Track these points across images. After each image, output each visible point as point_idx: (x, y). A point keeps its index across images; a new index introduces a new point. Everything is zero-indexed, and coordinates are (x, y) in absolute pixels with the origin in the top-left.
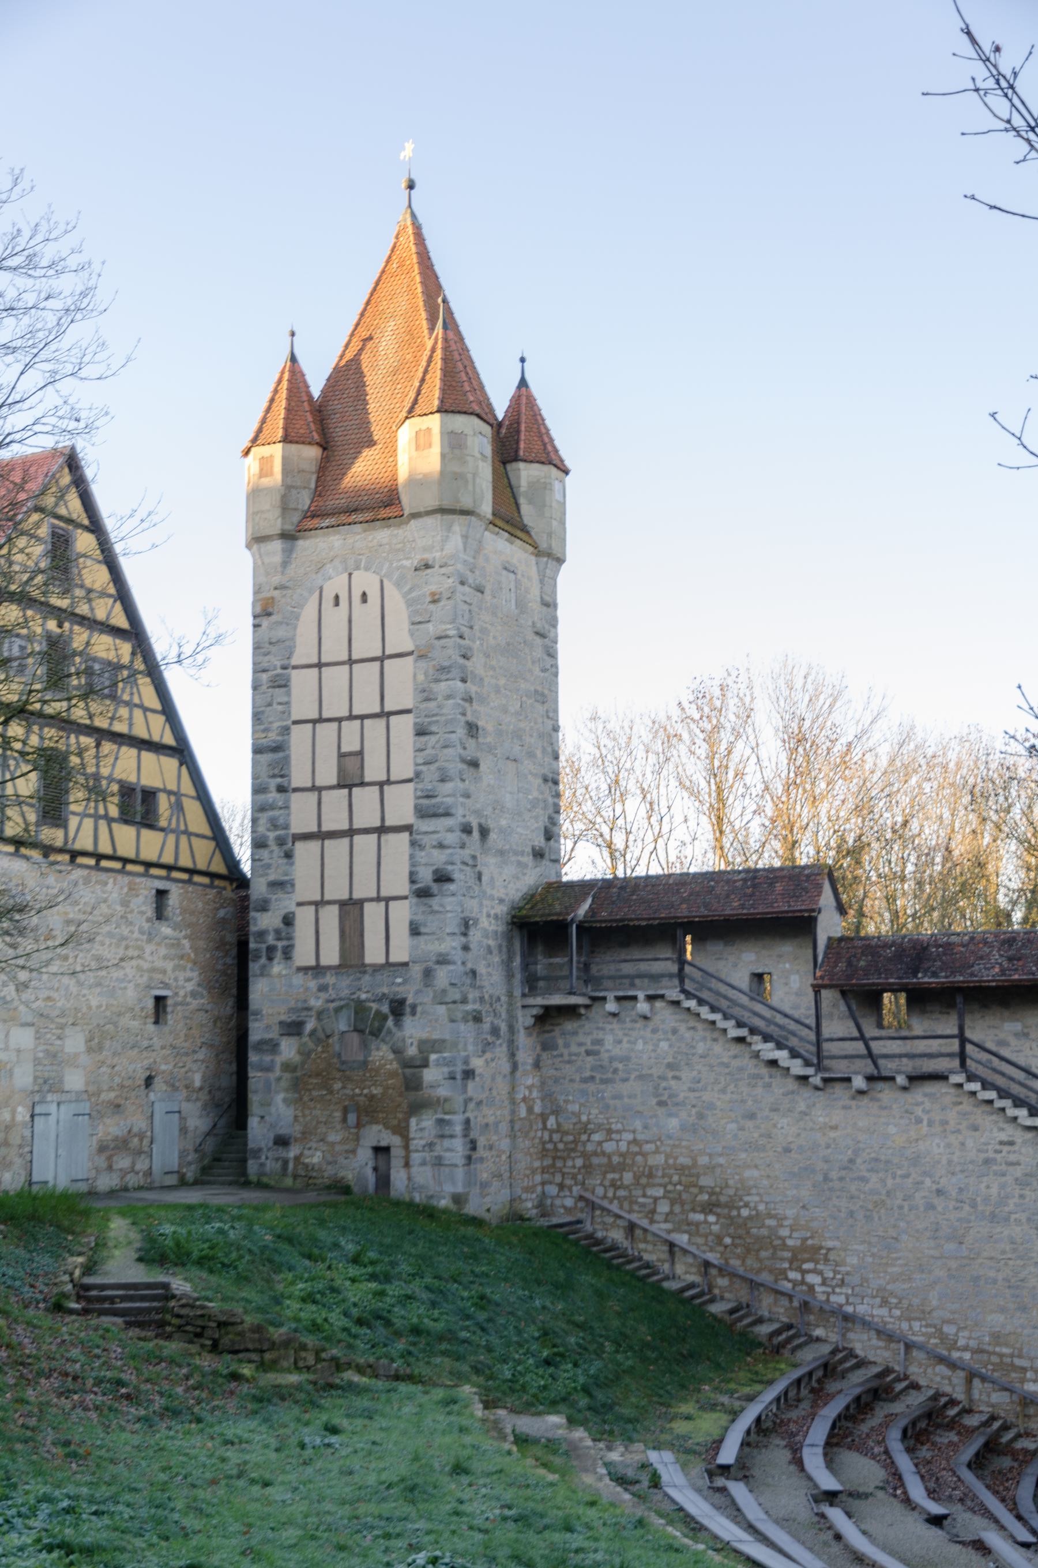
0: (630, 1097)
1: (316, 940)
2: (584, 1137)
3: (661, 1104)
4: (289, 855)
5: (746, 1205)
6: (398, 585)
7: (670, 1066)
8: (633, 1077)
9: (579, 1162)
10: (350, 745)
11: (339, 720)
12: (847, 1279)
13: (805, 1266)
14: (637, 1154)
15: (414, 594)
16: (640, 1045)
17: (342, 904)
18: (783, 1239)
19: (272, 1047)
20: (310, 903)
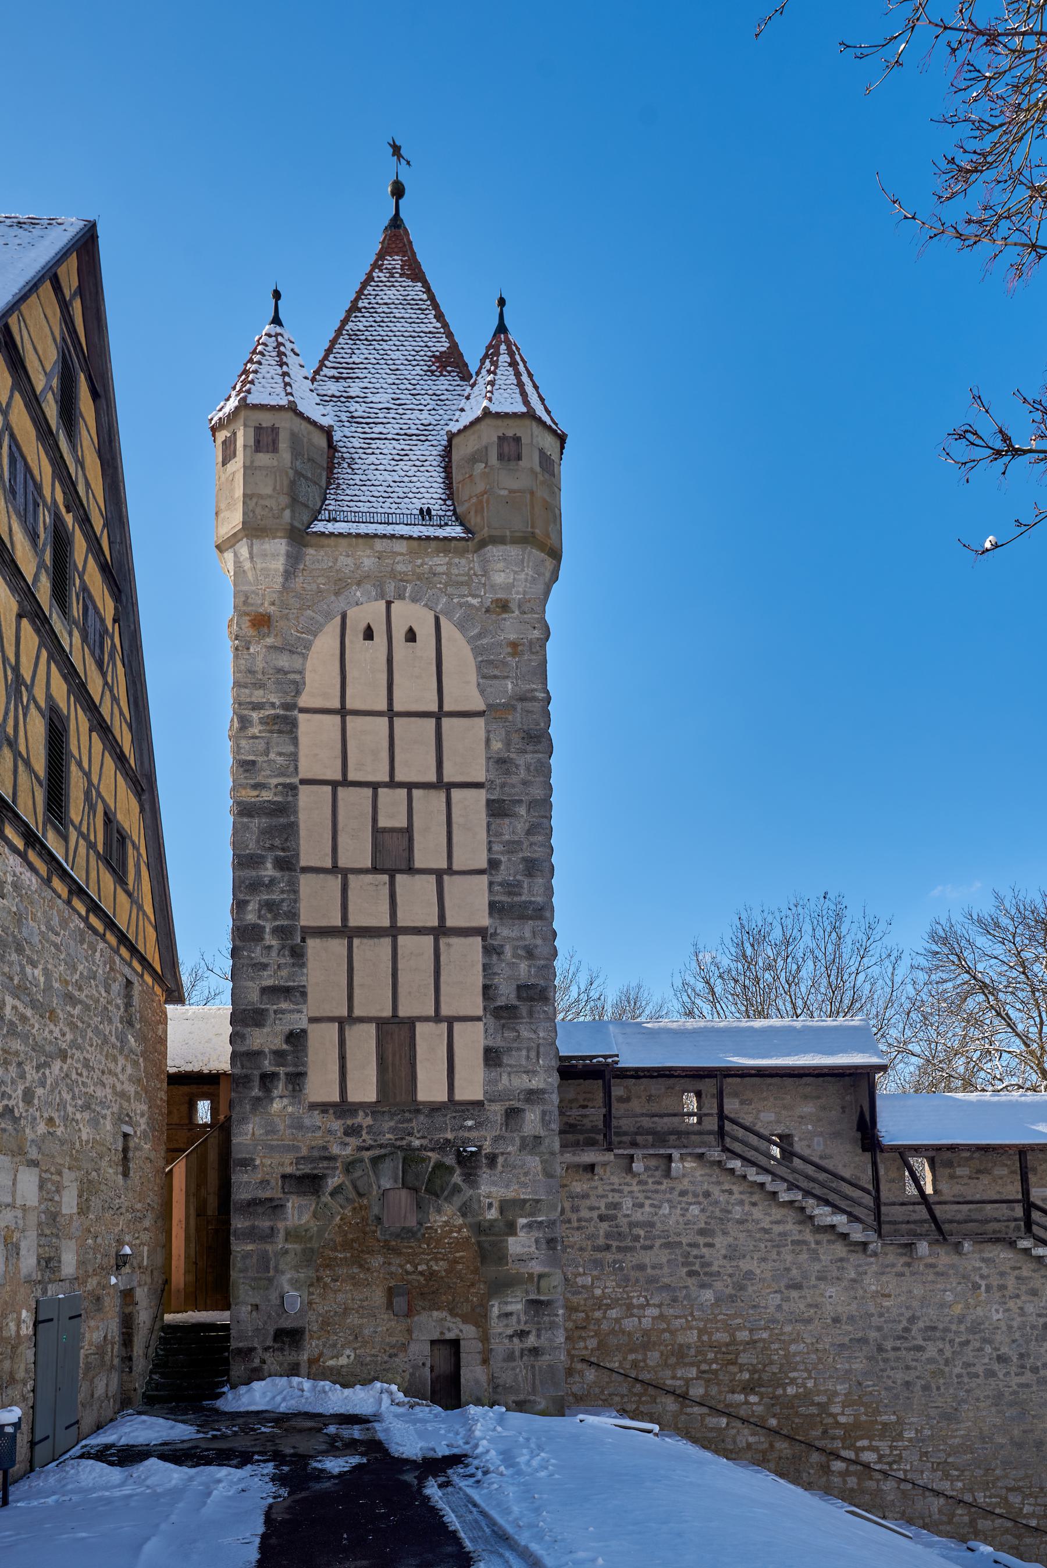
0: (653, 1268)
1: (343, 1070)
2: (598, 1314)
3: (691, 1274)
4: (298, 954)
5: (793, 1381)
6: (461, 626)
7: (702, 1232)
8: (657, 1245)
9: (592, 1343)
10: (392, 816)
11: (375, 786)
12: (904, 1454)
13: (859, 1444)
14: (664, 1330)
15: (485, 641)
16: (666, 1209)
17: (381, 1023)
18: (834, 1416)
19: (275, 1207)
20: (331, 1019)
